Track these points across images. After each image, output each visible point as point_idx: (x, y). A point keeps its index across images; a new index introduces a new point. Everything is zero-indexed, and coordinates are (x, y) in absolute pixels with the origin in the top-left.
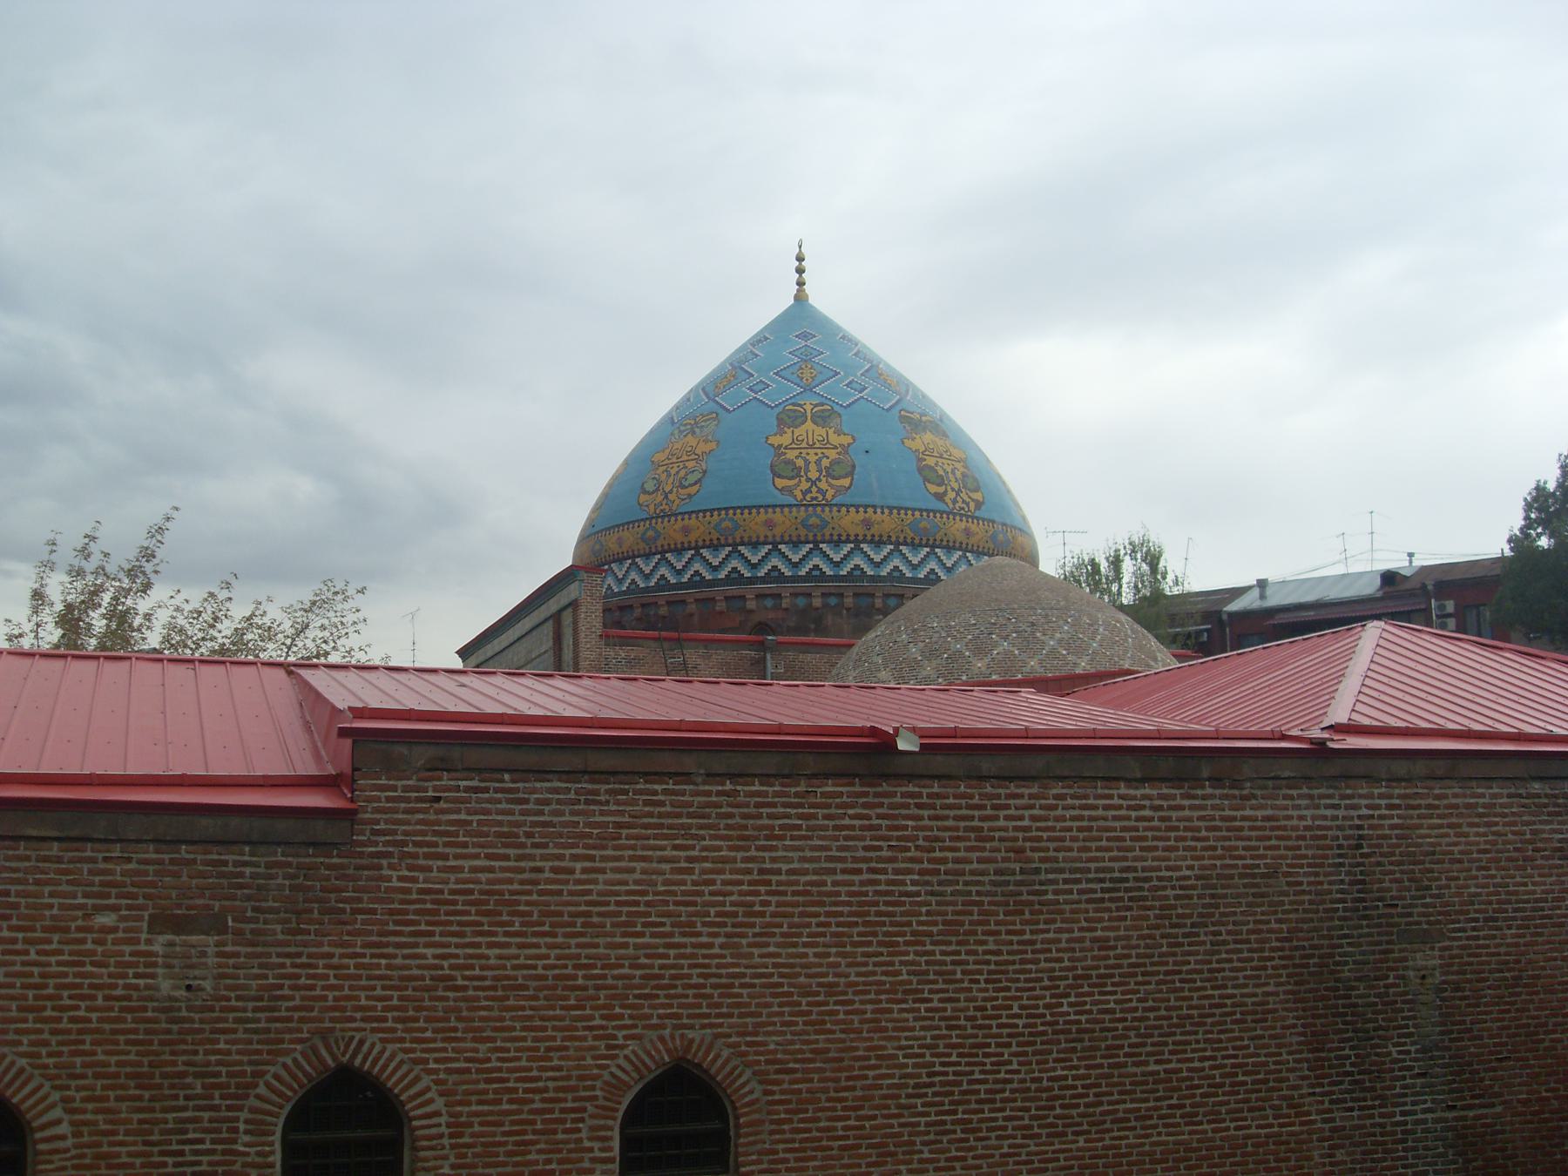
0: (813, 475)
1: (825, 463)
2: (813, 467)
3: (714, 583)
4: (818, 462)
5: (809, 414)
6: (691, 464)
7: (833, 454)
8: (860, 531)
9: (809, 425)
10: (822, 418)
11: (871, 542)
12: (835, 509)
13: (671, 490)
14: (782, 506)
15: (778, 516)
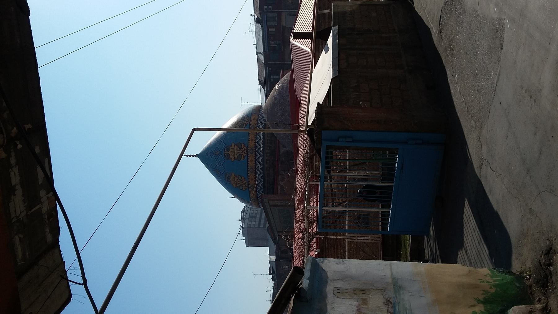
0: (241, 151)
1: (238, 149)
2: (239, 152)
3: (264, 173)
4: (238, 150)
5: (227, 153)
6: (237, 179)
7: (236, 147)
8: (253, 142)
9: (229, 153)
10: (228, 150)
11: (256, 139)
12: (249, 147)
13: (243, 183)
14: (248, 158)
15: (250, 159)
